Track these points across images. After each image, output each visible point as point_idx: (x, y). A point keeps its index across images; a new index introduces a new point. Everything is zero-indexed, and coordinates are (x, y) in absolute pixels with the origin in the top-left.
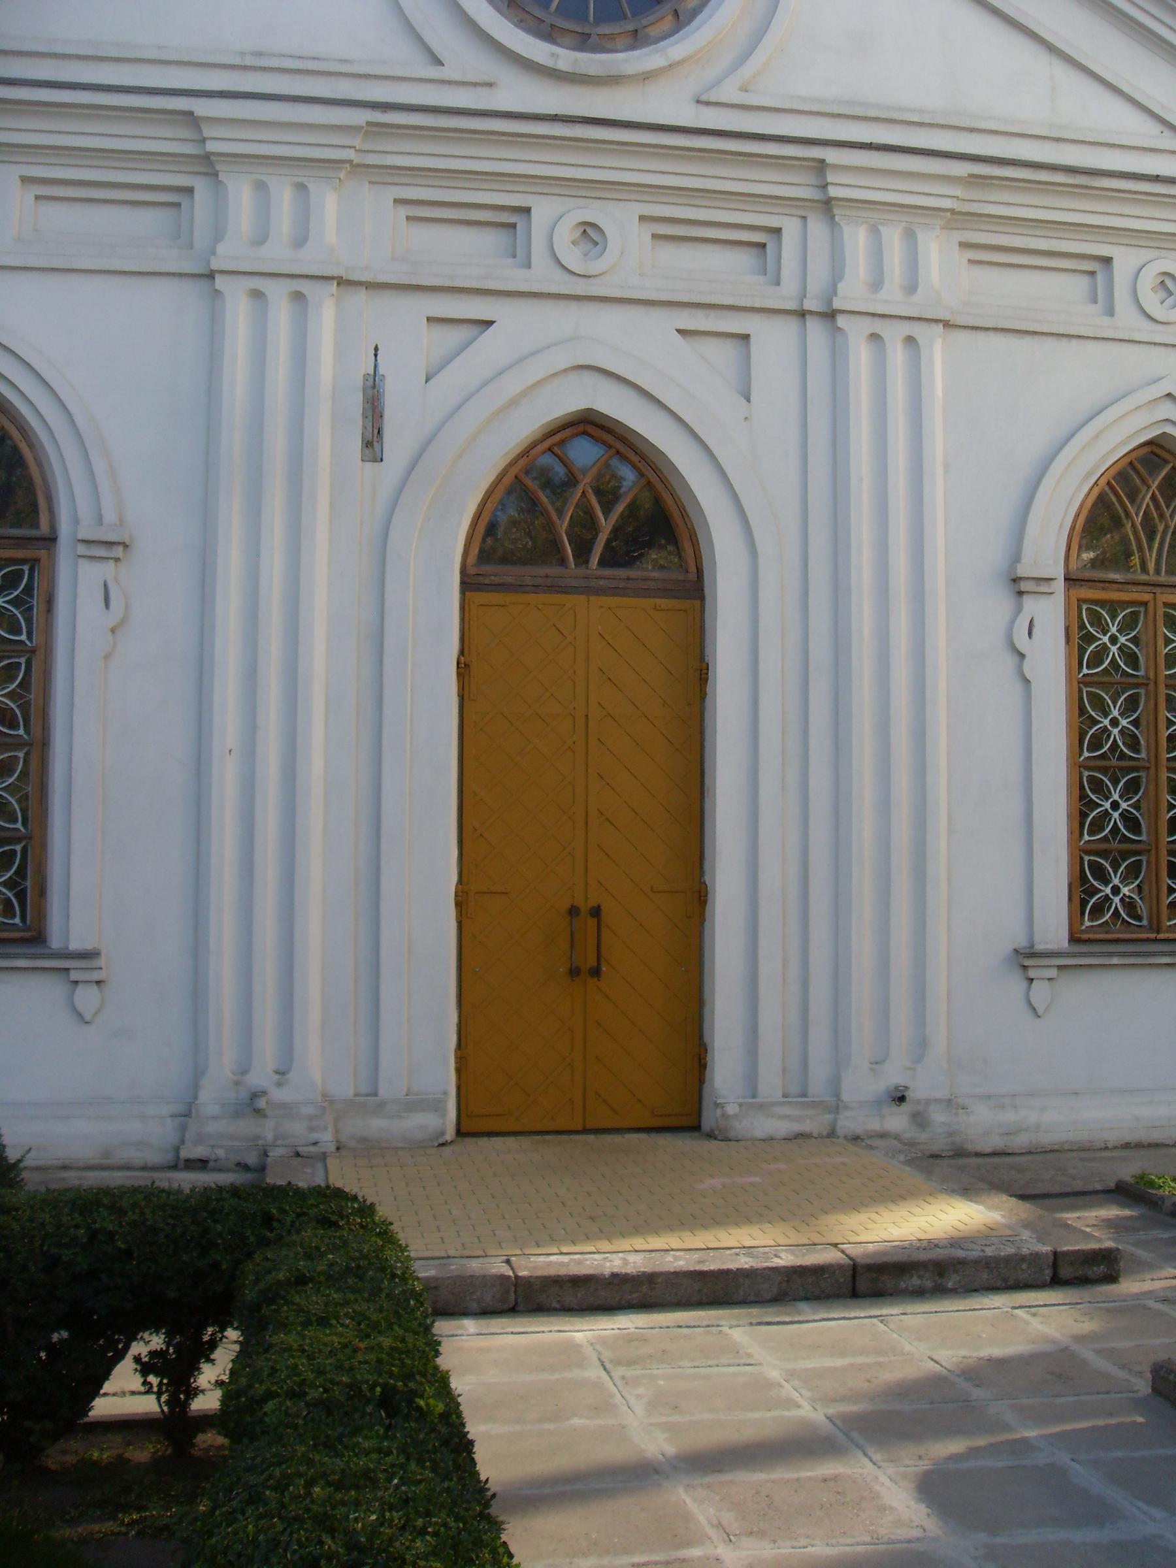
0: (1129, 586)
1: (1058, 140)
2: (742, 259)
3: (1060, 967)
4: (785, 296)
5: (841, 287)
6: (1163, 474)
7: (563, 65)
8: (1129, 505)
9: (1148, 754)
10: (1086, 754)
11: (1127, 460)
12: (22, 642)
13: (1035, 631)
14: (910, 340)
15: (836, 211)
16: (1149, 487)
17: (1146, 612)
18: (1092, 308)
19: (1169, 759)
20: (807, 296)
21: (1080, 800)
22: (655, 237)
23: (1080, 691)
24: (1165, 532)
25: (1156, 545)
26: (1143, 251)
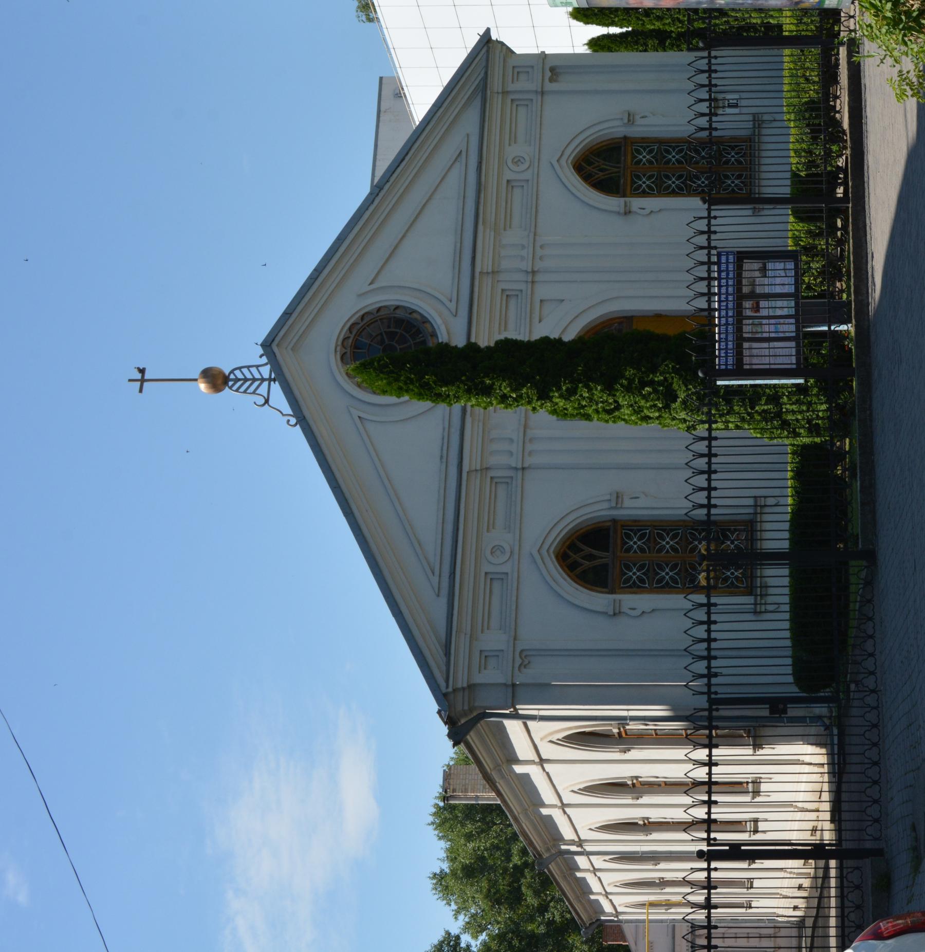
10: (685, 192)
12: (649, 532)
14: (542, 247)
16: (590, 170)
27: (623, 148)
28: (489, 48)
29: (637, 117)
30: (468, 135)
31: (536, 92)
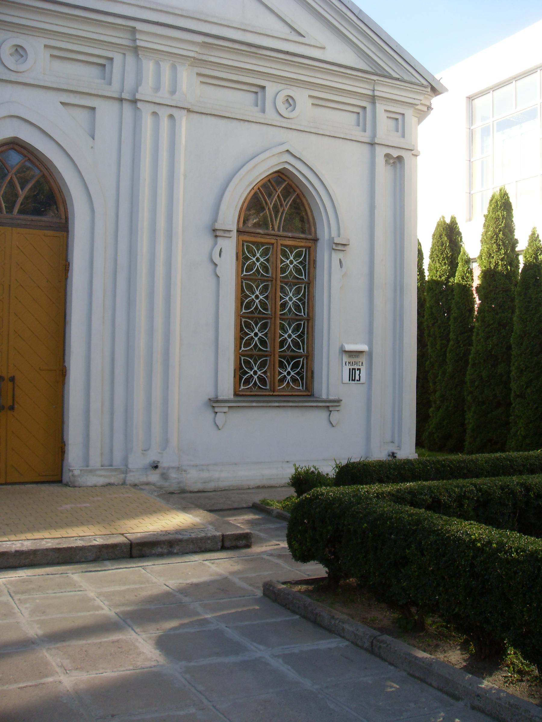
0: (266, 236)
1: (244, 30)
2: (94, 71)
3: (229, 407)
4: (113, 90)
5: (140, 89)
6: (283, 186)
8: (268, 200)
9: (271, 311)
10: (244, 311)
11: (267, 179)
14: (171, 116)
15: (140, 52)
16: (277, 191)
17: (273, 248)
18: (256, 109)
19: (281, 314)
20: (124, 91)
21: (240, 332)
22: (52, 56)
23: (242, 282)
24: (282, 214)
25: (278, 219)
26: (280, 85)
27: (302, 236)
28: (425, 87)
29: (341, 255)
30: (324, 48)
31: (374, 135)
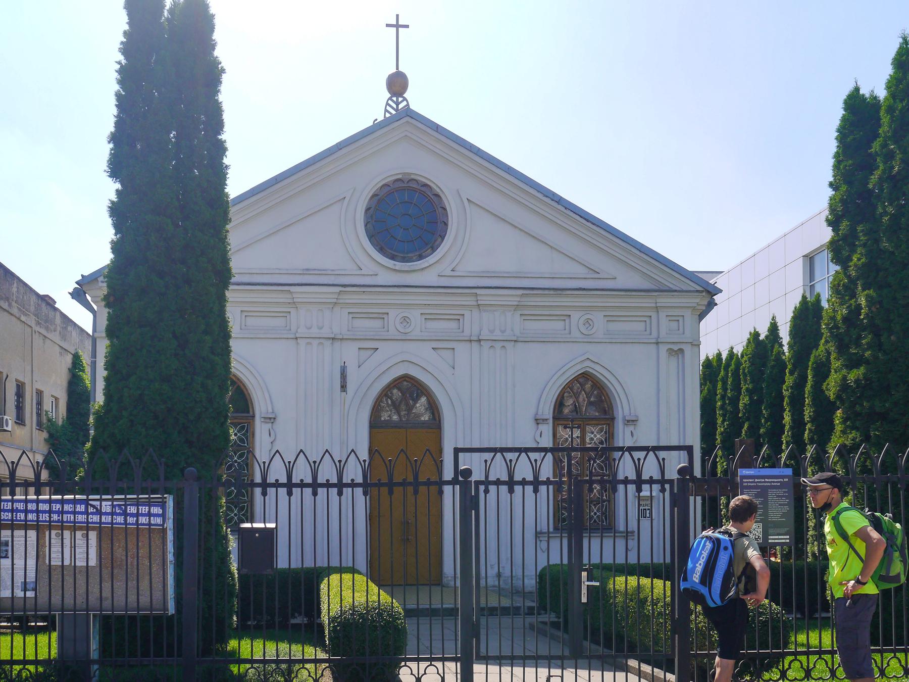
7: (397, 268)
13: (542, 435)
29: (632, 428)
30: (615, 278)
